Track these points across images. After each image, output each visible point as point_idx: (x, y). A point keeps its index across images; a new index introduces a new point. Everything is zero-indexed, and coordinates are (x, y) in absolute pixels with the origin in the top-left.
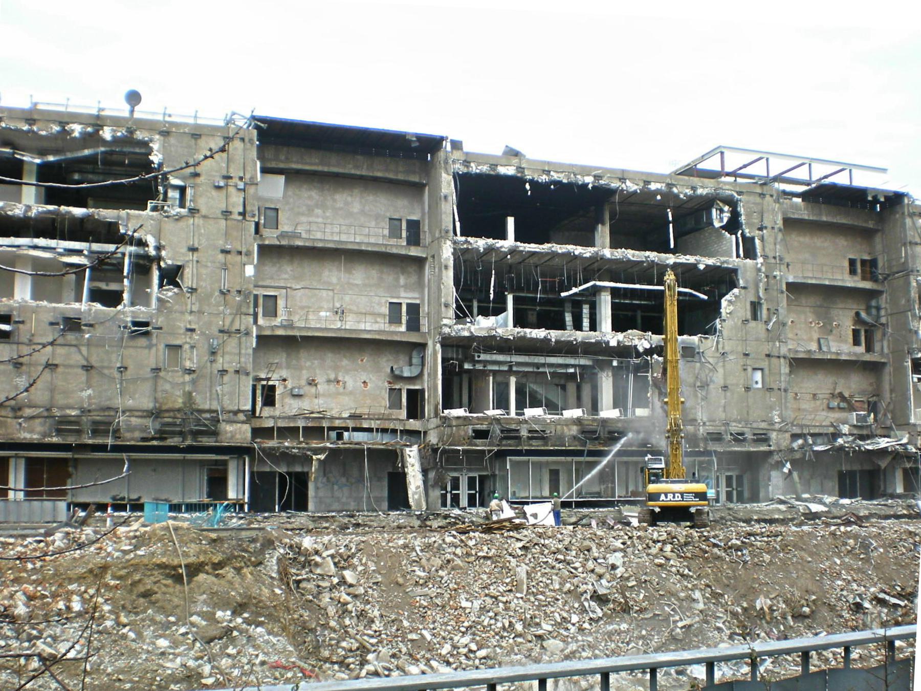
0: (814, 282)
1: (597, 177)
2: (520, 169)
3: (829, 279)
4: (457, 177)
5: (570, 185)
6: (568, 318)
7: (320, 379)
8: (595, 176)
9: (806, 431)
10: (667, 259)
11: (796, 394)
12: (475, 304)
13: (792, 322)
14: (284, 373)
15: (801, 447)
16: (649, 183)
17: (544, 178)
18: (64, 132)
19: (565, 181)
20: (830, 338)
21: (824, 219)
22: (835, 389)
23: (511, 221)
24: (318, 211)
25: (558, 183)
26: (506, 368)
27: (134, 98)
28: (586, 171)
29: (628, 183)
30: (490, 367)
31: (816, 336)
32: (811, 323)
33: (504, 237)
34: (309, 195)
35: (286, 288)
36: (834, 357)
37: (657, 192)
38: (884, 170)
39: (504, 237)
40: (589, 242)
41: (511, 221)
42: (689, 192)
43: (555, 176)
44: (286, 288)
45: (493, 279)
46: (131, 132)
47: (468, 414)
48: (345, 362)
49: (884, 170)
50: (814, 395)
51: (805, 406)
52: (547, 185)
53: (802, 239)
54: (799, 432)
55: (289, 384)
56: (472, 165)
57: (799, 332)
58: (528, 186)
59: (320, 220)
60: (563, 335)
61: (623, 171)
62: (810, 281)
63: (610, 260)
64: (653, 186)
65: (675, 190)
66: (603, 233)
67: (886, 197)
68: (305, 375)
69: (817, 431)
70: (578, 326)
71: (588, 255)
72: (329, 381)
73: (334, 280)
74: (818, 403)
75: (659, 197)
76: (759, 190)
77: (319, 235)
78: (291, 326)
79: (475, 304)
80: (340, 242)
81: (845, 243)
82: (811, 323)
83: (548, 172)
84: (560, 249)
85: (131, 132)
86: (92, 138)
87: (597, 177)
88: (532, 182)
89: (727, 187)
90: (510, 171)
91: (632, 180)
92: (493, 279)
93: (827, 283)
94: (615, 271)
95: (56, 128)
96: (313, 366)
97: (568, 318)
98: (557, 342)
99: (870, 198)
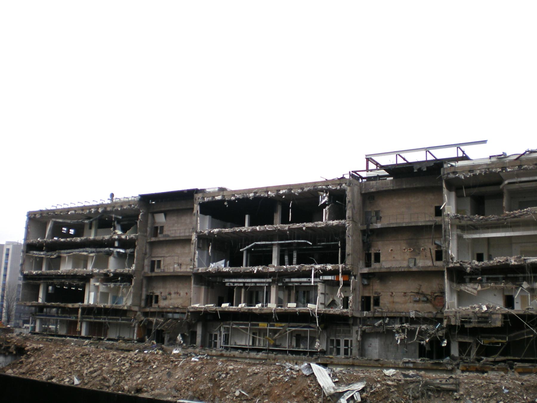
0: (395, 226)
1: (255, 193)
2: (223, 196)
3: (415, 222)
4: (200, 204)
5: (243, 199)
6: (286, 258)
7: (172, 292)
8: (254, 193)
9: (385, 315)
10: (285, 227)
11: (392, 293)
12: (295, 255)
13: (392, 250)
14: (161, 290)
15: (380, 325)
16: (280, 191)
17: (233, 198)
18: (90, 212)
19: (241, 198)
20: (417, 258)
21: (404, 187)
22: (419, 289)
23: (247, 217)
24: (176, 225)
25: (238, 199)
26: (242, 285)
27: (112, 195)
28: (250, 191)
29: (269, 193)
30: (236, 285)
31: (407, 257)
32: (405, 250)
33: (244, 225)
34: (173, 219)
35: (163, 257)
36: (406, 270)
37: (283, 194)
38: (484, 142)
39: (244, 225)
40: (272, 223)
41: (247, 217)
42: (300, 191)
43: (238, 196)
44: (163, 257)
45: (259, 243)
46: (106, 208)
47: (211, 306)
48: (181, 285)
49: (484, 142)
50: (405, 293)
51: (396, 299)
52: (234, 201)
53: (400, 200)
54: (380, 315)
55: (163, 294)
56: (205, 198)
57: (395, 256)
58: (226, 203)
59: (176, 228)
60: (235, 269)
61: (267, 187)
62: (392, 226)
63: (259, 231)
64: (281, 192)
65: (293, 192)
66: (277, 217)
67: (427, 168)
68: (168, 291)
69: (392, 315)
70: (291, 263)
71: (249, 230)
72: (175, 293)
73: (179, 252)
74: (407, 298)
75: (284, 197)
76: (338, 182)
77: (178, 235)
78: (164, 272)
79: (295, 255)
80: (175, 237)
81: (433, 197)
82: (405, 250)
83: (234, 195)
84: (227, 230)
85: (106, 208)
86: (97, 212)
87: (255, 193)
88: (230, 202)
89: (320, 184)
90: (219, 198)
91: (271, 191)
92: (259, 243)
93: (404, 225)
94: (281, 235)
95: (88, 211)
96: (171, 287)
97: (286, 258)
98: (233, 272)
99: (415, 171)
